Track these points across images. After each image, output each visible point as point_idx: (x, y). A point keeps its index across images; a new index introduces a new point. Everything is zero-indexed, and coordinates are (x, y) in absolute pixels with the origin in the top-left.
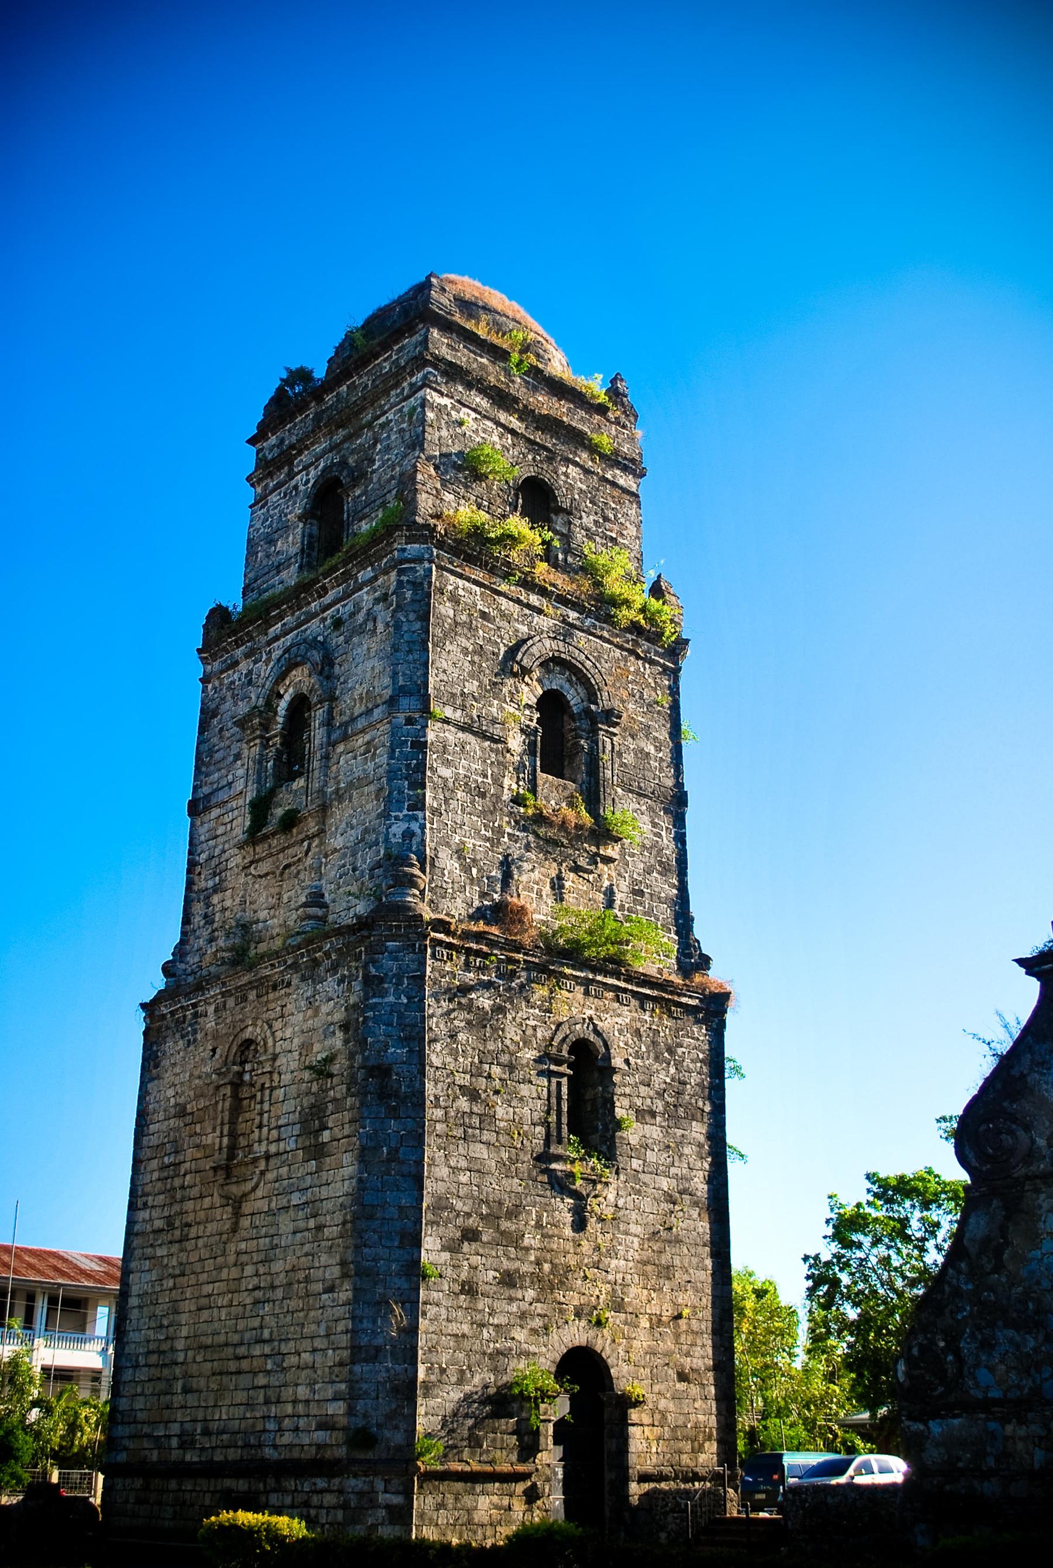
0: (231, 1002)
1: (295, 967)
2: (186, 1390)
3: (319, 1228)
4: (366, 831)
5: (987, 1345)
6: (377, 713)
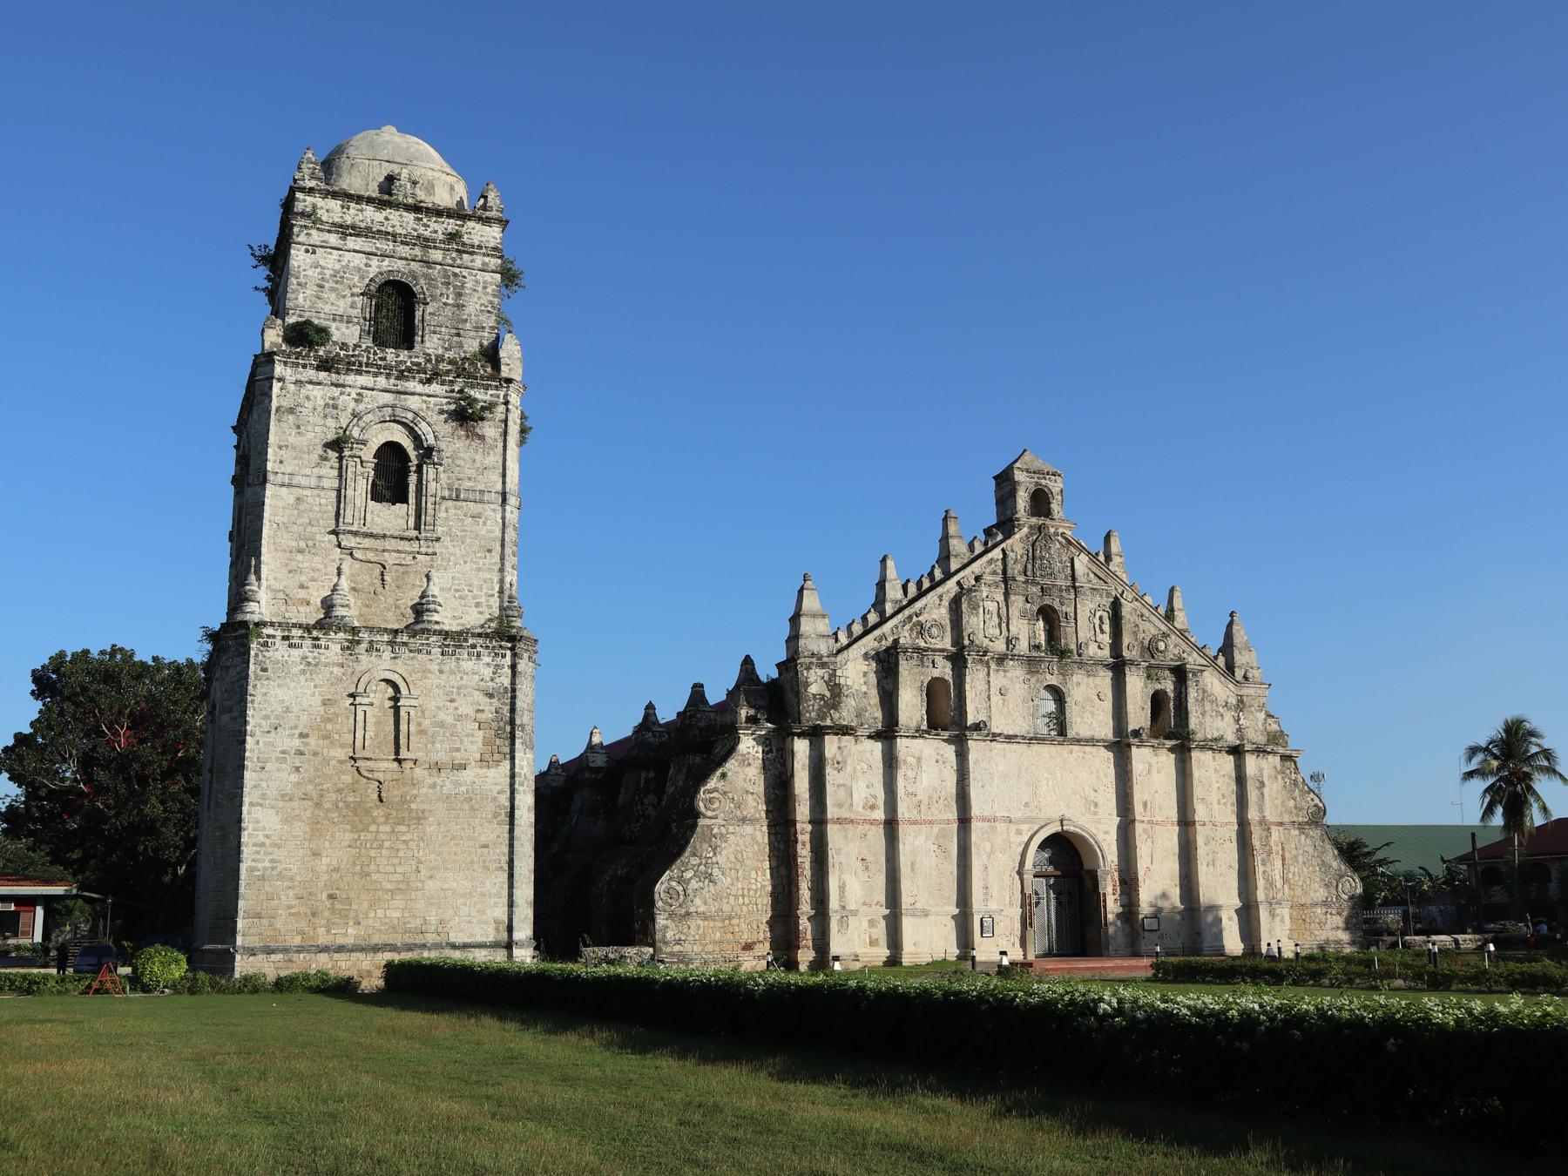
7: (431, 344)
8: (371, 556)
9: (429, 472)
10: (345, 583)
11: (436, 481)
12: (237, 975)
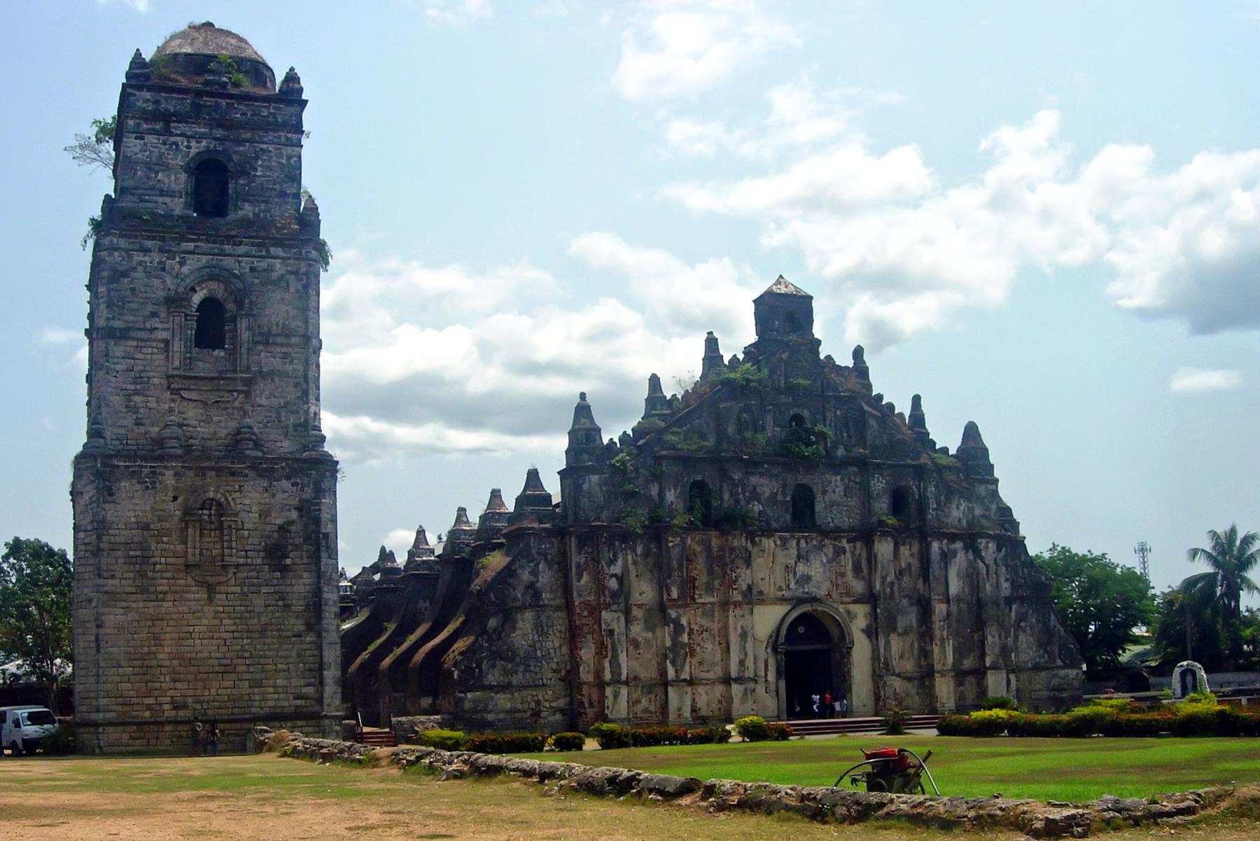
0: (190, 473)
1: (253, 468)
3: (287, 606)
4: (287, 404)
5: (493, 666)
6: (294, 340)
8: (194, 395)
9: (243, 324)
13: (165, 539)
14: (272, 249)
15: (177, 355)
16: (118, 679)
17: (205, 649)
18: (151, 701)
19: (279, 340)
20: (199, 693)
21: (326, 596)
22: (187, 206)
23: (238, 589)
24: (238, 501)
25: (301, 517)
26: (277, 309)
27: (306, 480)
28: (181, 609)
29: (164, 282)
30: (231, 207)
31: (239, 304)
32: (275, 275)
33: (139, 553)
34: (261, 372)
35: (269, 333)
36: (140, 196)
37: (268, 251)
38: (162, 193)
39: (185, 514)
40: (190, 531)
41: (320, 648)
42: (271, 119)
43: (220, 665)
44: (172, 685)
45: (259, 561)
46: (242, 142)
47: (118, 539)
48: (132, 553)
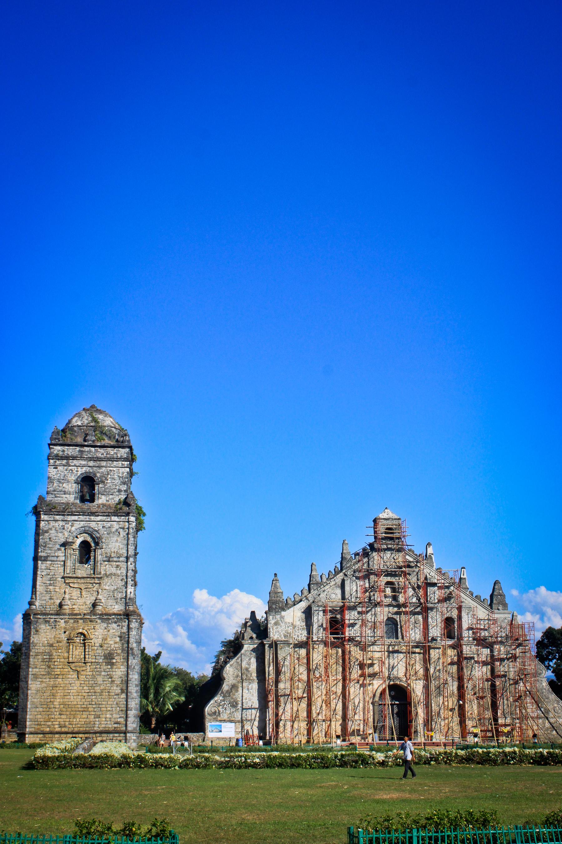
0: (72, 621)
2: (60, 714)
3: (113, 681)
4: (118, 588)
6: (121, 559)
7: (101, 500)
8: (76, 586)
9: (99, 552)
10: (67, 596)
11: (100, 555)
12: (27, 742)
13: (60, 651)
14: (114, 518)
15: (69, 568)
16: (36, 713)
17: (74, 700)
18: (50, 723)
19: (115, 559)
20: (71, 720)
21: (130, 676)
22: (76, 498)
23: (91, 673)
24: (93, 633)
25: (121, 640)
26: (114, 544)
27: (124, 624)
28: (65, 682)
29: (64, 534)
30: (96, 498)
31: (97, 544)
32: (114, 530)
33: (48, 657)
34: (106, 574)
35: (110, 557)
36: (55, 494)
37: (111, 519)
38: (65, 493)
39: (68, 640)
40: (71, 647)
41: (127, 701)
42: (115, 456)
43: (81, 708)
44: (59, 716)
45: (101, 661)
46: (100, 467)
47: (39, 651)
48: (45, 657)
